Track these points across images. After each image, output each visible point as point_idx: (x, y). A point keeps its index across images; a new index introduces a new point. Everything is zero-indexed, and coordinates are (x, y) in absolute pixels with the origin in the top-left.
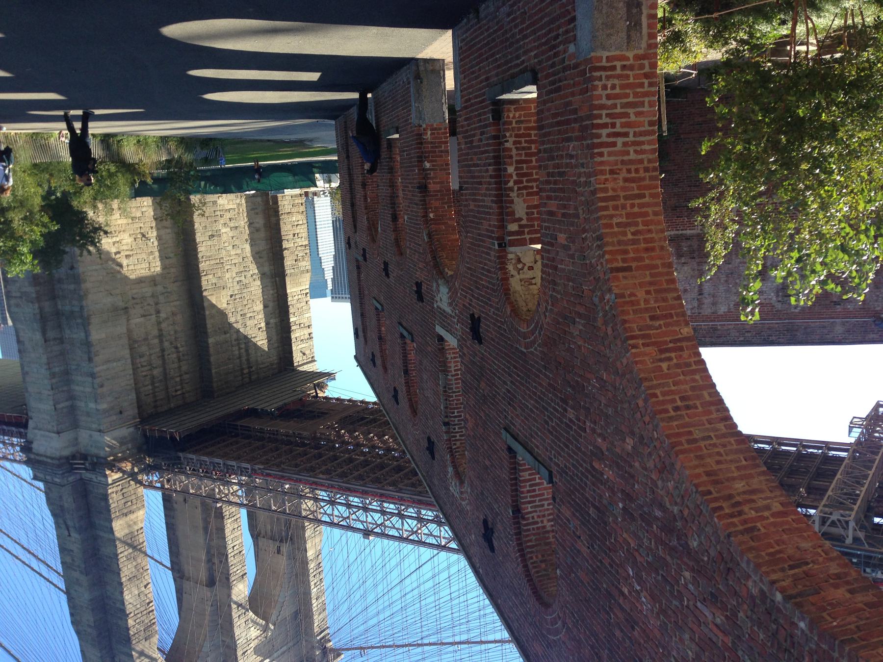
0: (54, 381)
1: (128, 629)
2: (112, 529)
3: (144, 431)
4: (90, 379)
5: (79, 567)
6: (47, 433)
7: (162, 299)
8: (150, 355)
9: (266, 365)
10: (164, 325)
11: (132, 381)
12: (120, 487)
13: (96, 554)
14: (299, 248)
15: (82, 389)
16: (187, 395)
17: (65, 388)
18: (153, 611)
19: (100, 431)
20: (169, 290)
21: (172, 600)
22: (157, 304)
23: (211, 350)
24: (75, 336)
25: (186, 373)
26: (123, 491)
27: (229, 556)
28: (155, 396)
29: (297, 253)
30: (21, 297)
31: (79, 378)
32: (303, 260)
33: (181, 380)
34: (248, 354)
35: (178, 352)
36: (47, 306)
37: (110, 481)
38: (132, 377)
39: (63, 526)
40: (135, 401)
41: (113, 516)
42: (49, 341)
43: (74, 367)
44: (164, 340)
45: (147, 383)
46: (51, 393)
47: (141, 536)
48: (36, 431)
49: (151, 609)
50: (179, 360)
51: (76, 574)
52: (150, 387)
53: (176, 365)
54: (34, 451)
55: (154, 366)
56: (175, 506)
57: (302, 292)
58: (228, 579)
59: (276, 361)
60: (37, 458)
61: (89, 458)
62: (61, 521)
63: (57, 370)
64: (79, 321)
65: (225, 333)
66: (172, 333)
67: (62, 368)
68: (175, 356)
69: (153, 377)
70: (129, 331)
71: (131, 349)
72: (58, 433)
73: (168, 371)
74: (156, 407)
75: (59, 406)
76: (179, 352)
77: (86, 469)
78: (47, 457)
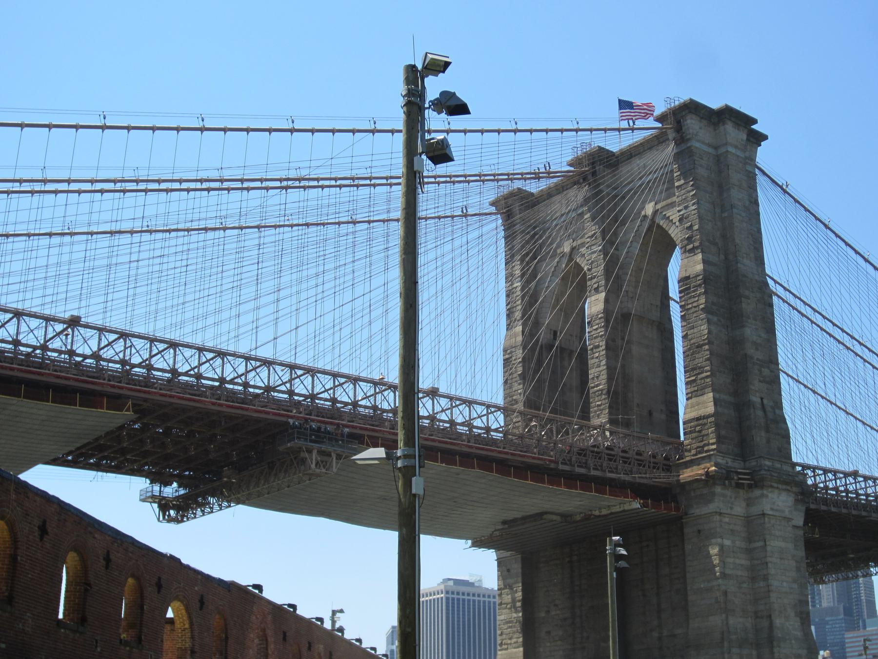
2: (715, 404)
3: (677, 509)
4: (728, 572)
6: (777, 514)
15: (738, 561)
17: (756, 562)
19: (720, 514)
24: (741, 620)
31: (739, 573)
39: (768, 409)
43: (745, 585)
46: (769, 559)
51: (758, 355)
60: (789, 488)
63: (762, 584)
64: (734, 637)
72: (764, 514)
75: (761, 544)
78: (777, 488)
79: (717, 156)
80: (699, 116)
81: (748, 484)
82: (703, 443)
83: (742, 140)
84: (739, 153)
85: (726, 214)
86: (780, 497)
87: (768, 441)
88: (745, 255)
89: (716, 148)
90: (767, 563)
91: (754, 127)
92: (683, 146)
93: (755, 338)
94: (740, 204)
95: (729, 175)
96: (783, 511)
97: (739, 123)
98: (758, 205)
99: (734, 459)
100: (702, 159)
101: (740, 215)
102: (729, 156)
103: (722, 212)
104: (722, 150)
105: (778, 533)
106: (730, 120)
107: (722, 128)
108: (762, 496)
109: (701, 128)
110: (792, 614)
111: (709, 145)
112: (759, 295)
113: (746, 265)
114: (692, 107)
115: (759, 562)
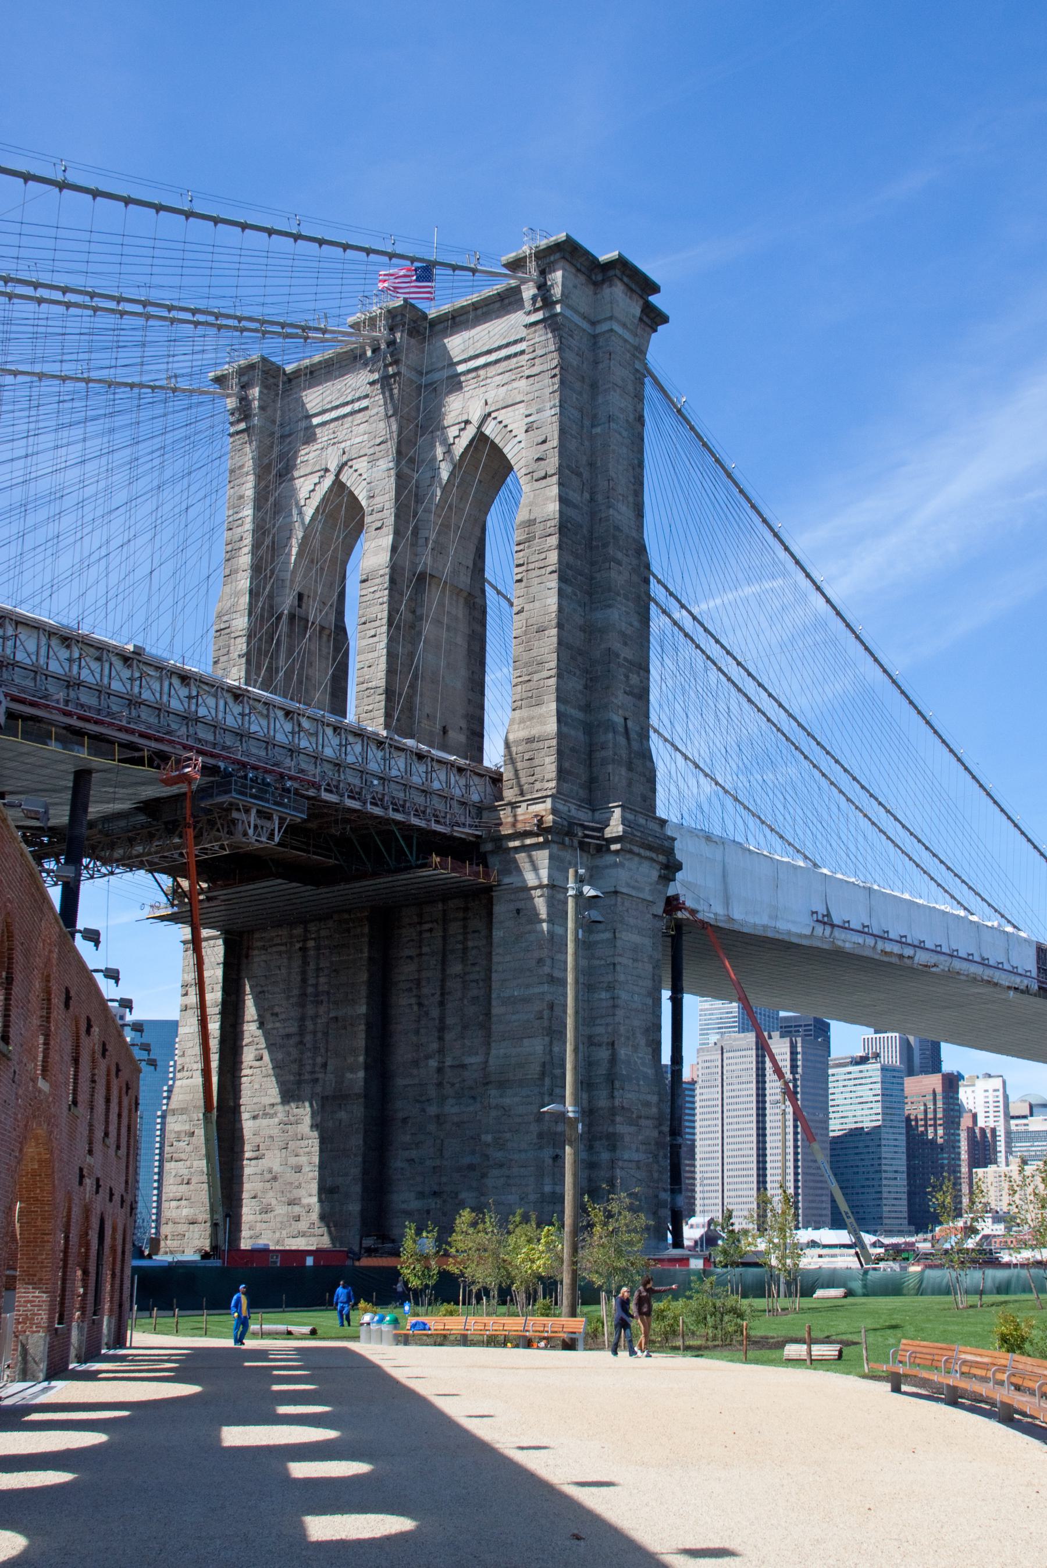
0: (610, 978)
1: (560, 547)
2: (559, 721)
3: (487, 875)
5: (619, 665)
6: (634, 893)
7: (432, 1092)
8: (461, 999)
9: (274, 949)
10: (435, 1046)
11: (495, 959)
12: (538, 785)
13: (591, 679)
14: (183, 1156)
16: (416, 919)
17: (597, 962)
18: (518, 566)
20: (418, 1105)
21: (495, 553)
22: (440, 1085)
23: (364, 991)
25: (410, 958)
26: (533, 779)
27: (385, 621)
28: (465, 927)
29: (188, 1149)
30: (639, 1117)
32: (179, 1132)
33: (420, 947)
34: (304, 973)
35: (418, 997)
36: (603, 1103)
37: (549, 803)
38: (494, 968)
39: (633, 735)
40: (495, 926)
41: (554, 742)
42: (608, 1044)
44: (437, 1021)
45: (474, 952)
46: (618, 959)
47: (518, 697)
48: (650, 898)
49: (520, 569)
50: (418, 983)
51: (626, 653)
52: (470, 944)
53: (425, 974)
54: (658, 867)
55: (459, 980)
56: (463, 724)
57: (189, 1074)
58: (392, 581)
59: (256, 952)
60: (654, 855)
61: (576, 843)
62: (635, 746)
63: (603, 995)
65: (336, 1018)
66: (422, 1031)
67: (596, 996)
68: (425, 991)
69: (464, 960)
70: (488, 1044)
71: (488, 1014)
72: (616, 892)
73: (439, 967)
74: (466, 909)
75: (607, 935)
76: (416, 996)
77: (585, 827)
78: (638, 855)
79: (595, 337)
80: (575, 266)
81: (597, 844)
82: (534, 778)
83: (634, 316)
84: (627, 336)
85: (598, 430)
87: (630, 784)
88: (621, 498)
89: (593, 324)
90: (614, 964)
91: (653, 299)
93: (624, 626)
94: (621, 416)
95: (610, 367)
97: (633, 286)
99: (580, 806)
100: (571, 336)
101: (620, 434)
102: (613, 338)
103: (593, 426)
104: (604, 327)
105: (632, 921)
106: (621, 280)
107: (606, 291)
109: (575, 287)
110: (643, 1042)
111: (584, 317)
112: (635, 562)
113: (621, 513)
115: (603, 962)
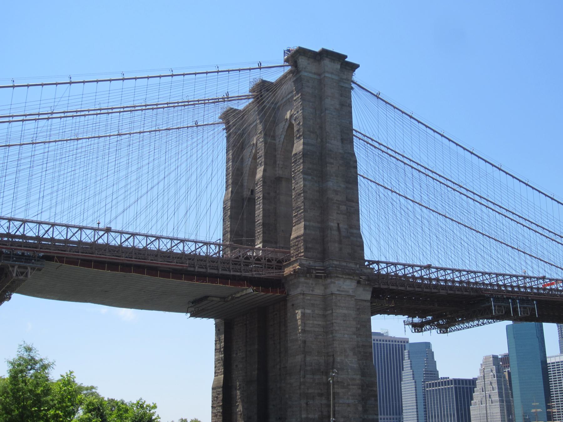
15: (315, 322)
17: (328, 323)
31: (317, 329)
43: (320, 337)
60: (352, 277)
78: (342, 278)
82: (298, 252)
86: (345, 283)
90: (333, 323)
92: (298, 76)
96: (348, 292)
98: (351, 107)
99: (315, 261)
100: (308, 82)
104: (323, 76)
108: (332, 282)
109: (309, 64)
111: (315, 74)
114: (301, 52)
